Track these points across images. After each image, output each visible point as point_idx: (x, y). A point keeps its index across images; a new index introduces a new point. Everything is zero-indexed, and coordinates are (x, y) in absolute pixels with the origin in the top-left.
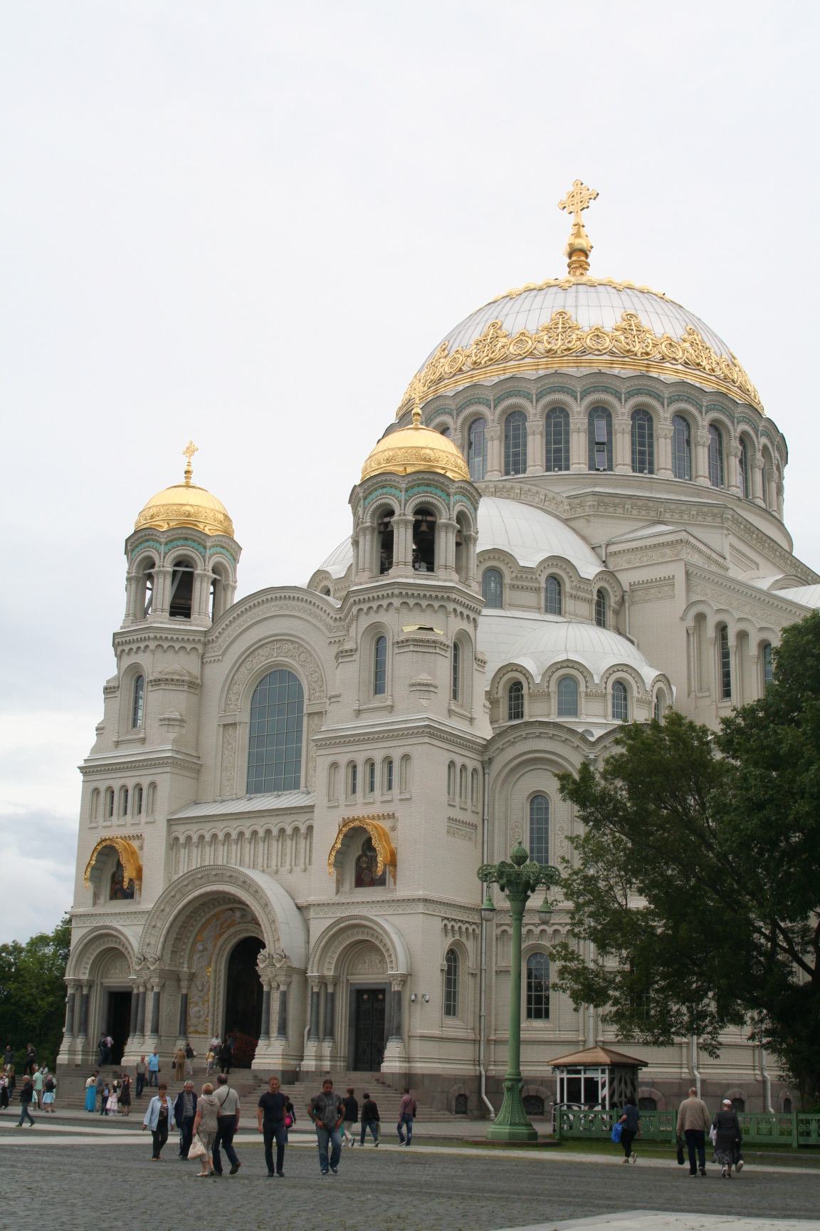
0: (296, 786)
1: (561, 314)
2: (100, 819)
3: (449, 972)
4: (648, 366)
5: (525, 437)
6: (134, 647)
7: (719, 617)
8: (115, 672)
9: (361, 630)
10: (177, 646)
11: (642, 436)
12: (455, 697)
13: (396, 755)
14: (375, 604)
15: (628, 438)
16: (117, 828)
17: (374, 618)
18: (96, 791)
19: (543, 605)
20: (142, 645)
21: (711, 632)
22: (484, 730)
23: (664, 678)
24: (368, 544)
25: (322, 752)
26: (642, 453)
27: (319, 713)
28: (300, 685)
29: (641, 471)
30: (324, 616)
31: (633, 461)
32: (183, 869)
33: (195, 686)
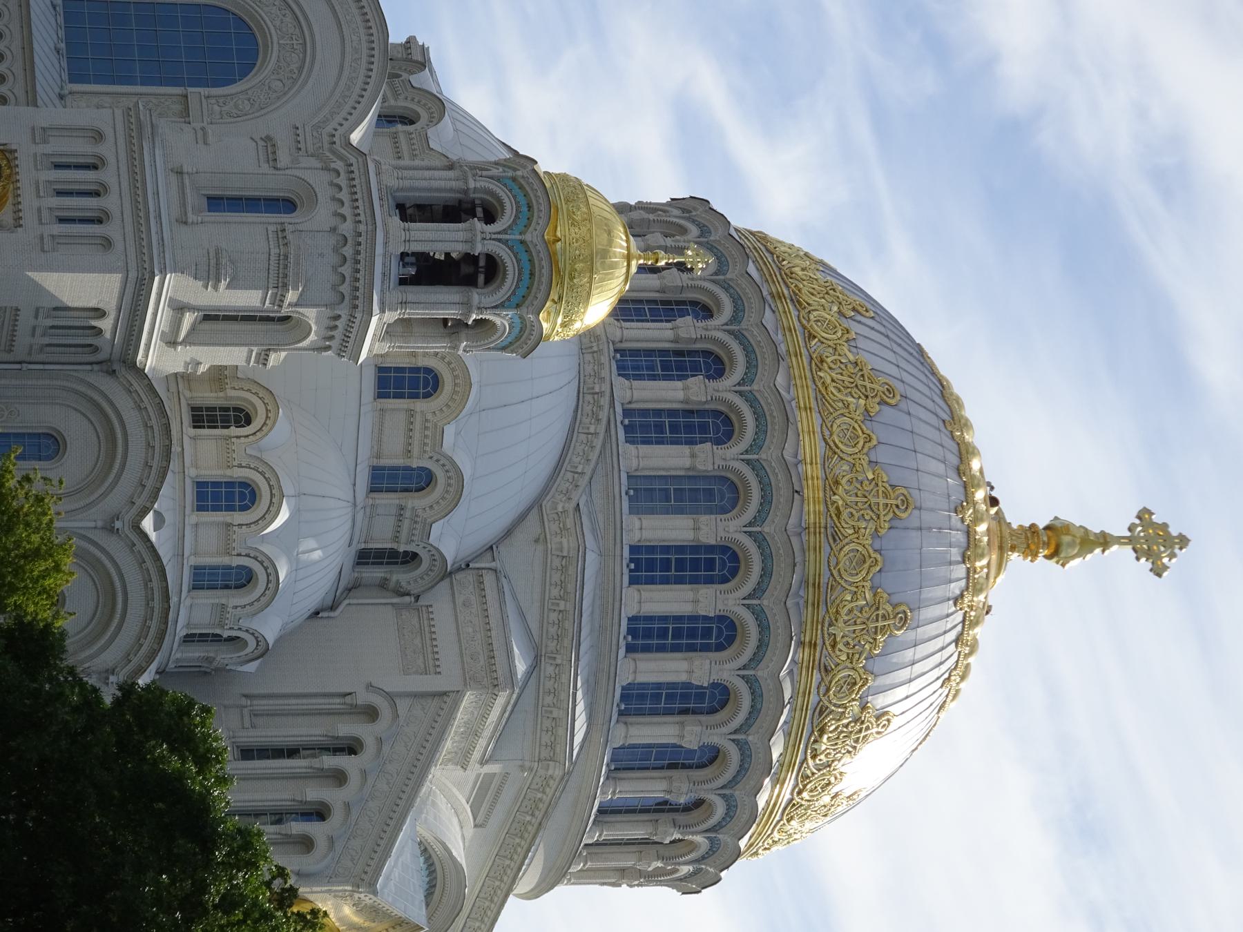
0: (77, 75)
1: (906, 501)
4: (813, 645)
5: (691, 442)
9: (308, 176)
11: (692, 633)
12: (207, 318)
13: (110, 230)
14: (344, 195)
15: (685, 609)
17: (324, 193)
19: (385, 462)
21: (346, 729)
22: (155, 358)
23: (263, 651)
26: (663, 633)
27: (185, 112)
29: (632, 631)
30: (339, 119)
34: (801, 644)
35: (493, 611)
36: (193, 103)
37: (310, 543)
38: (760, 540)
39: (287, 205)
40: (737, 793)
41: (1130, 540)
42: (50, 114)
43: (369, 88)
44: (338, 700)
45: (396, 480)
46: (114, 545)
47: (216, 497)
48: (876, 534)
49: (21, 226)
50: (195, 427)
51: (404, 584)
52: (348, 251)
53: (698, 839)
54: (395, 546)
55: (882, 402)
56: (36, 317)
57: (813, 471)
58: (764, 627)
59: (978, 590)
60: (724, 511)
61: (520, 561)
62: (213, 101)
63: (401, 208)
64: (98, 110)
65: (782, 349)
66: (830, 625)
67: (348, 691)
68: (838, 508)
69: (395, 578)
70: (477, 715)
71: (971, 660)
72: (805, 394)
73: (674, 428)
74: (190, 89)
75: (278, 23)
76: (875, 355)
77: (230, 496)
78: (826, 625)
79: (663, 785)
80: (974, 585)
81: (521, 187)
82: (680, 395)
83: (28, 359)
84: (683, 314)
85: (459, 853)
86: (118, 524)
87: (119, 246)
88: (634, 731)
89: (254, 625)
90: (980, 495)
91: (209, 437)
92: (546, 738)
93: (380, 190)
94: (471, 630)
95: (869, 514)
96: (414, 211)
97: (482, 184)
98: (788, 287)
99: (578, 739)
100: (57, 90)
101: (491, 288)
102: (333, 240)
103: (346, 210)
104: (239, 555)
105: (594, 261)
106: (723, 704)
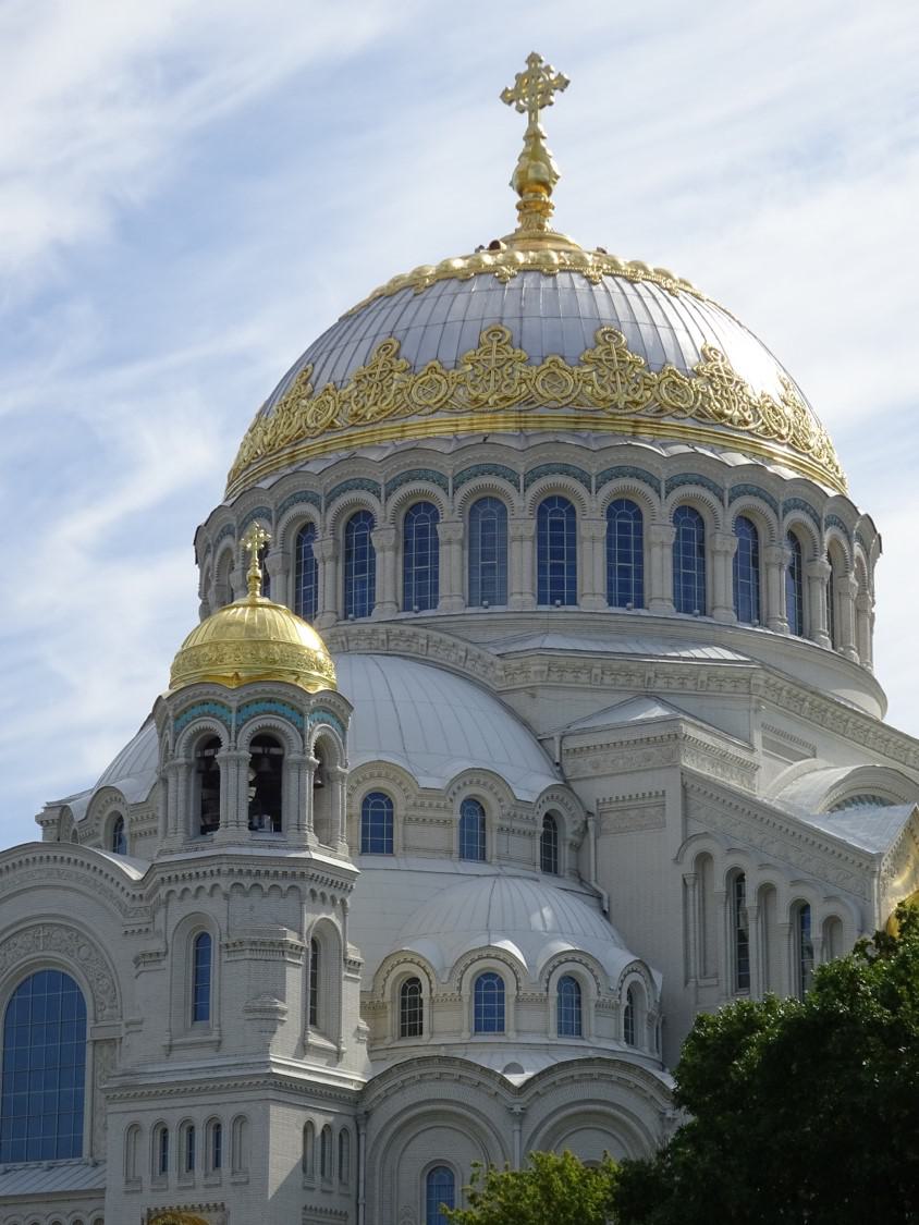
1: (494, 332)
4: (637, 424)
5: (436, 545)
7: (733, 861)
11: (625, 543)
12: (313, 1021)
13: (226, 1116)
14: (193, 886)
19: (456, 847)
21: (718, 884)
22: (353, 1072)
23: (642, 965)
24: (182, 783)
25: (117, 1107)
26: (625, 571)
28: (80, 995)
29: (622, 603)
30: (117, 892)
31: (610, 585)
34: (635, 436)
35: (602, 739)
36: (100, 1035)
37: (536, 920)
39: (202, 941)
43: (86, 861)
44: (691, 892)
45: (473, 835)
46: (539, 1112)
47: (489, 1012)
48: (527, 362)
49: (223, 1205)
50: (421, 1033)
51: (576, 828)
52: (247, 882)
53: (827, 537)
54: (538, 836)
55: (397, 355)
56: (312, 1189)
57: (465, 423)
58: (618, 472)
59: (582, 261)
60: (504, 511)
61: (555, 711)
62: (100, 1015)
64: (109, 1128)
65: (344, 454)
66: (616, 407)
67: (681, 881)
68: (501, 400)
69: (570, 836)
70: (705, 755)
71: (651, 268)
72: (389, 431)
73: (422, 560)
74: (88, 1038)
75: (23, 951)
76: (351, 362)
77: (489, 999)
78: (616, 411)
79: (774, 571)
80: (577, 265)
81: (185, 711)
82: (390, 554)
83: (354, 1198)
84: (310, 552)
85: (841, 772)
86: (517, 1109)
87: (242, 1108)
88: (721, 600)
89: (616, 974)
90: (488, 259)
91: (431, 1020)
92: (728, 686)
93: (187, 851)
94: (621, 762)
95: (507, 369)
96: (208, 816)
97: (181, 751)
98: (283, 449)
99: (729, 655)
100: (89, 1169)
101: (283, 740)
102: (237, 897)
103: (208, 884)
104: (547, 990)
105: (258, 640)
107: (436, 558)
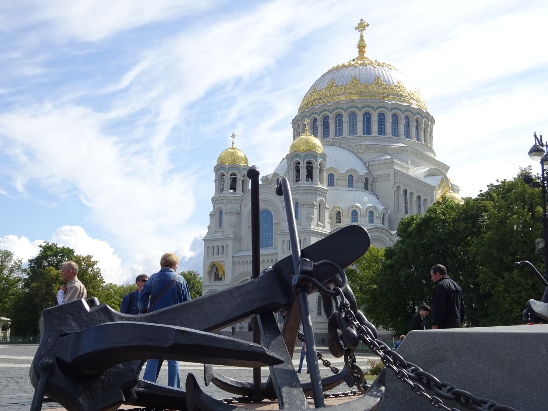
0: (271, 245)
2: (211, 257)
3: (319, 303)
4: (384, 97)
6: (219, 202)
8: (212, 209)
10: (233, 202)
11: (381, 122)
16: (216, 259)
18: (209, 247)
20: (222, 201)
21: (401, 192)
23: (386, 209)
26: (381, 128)
27: (278, 224)
29: (381, 134)
31: (378, 131)
32: (237, 272)
33: (239, 214)
34: (384, 99)
36: (276, 223)
37: (364, 199)
38: (362, 108)
40: (414, 112)
41: (362, 31)
42: (279, 251)
47: (355, 218)
52: (306, 192)
53: (424, 120)
57: (348, 97)
58: (380, 107)
59: (372, 63)
60: (356, 116)
61: (367, 157)
63: (297, 181)
72: (332, 99)
76: (324, 85)
79: (413, 128)
85: (428, 169)
87: (305, 237)
88: (401, 134)
89: (380, 211)
90: (353, 63)
96: (298, 179)
97: (292, 165)
99: (403, 145)
102: (304, 195)
103: (298, 192)
105: (307, 142)
106: (396, 115)
107: (342, 126)
